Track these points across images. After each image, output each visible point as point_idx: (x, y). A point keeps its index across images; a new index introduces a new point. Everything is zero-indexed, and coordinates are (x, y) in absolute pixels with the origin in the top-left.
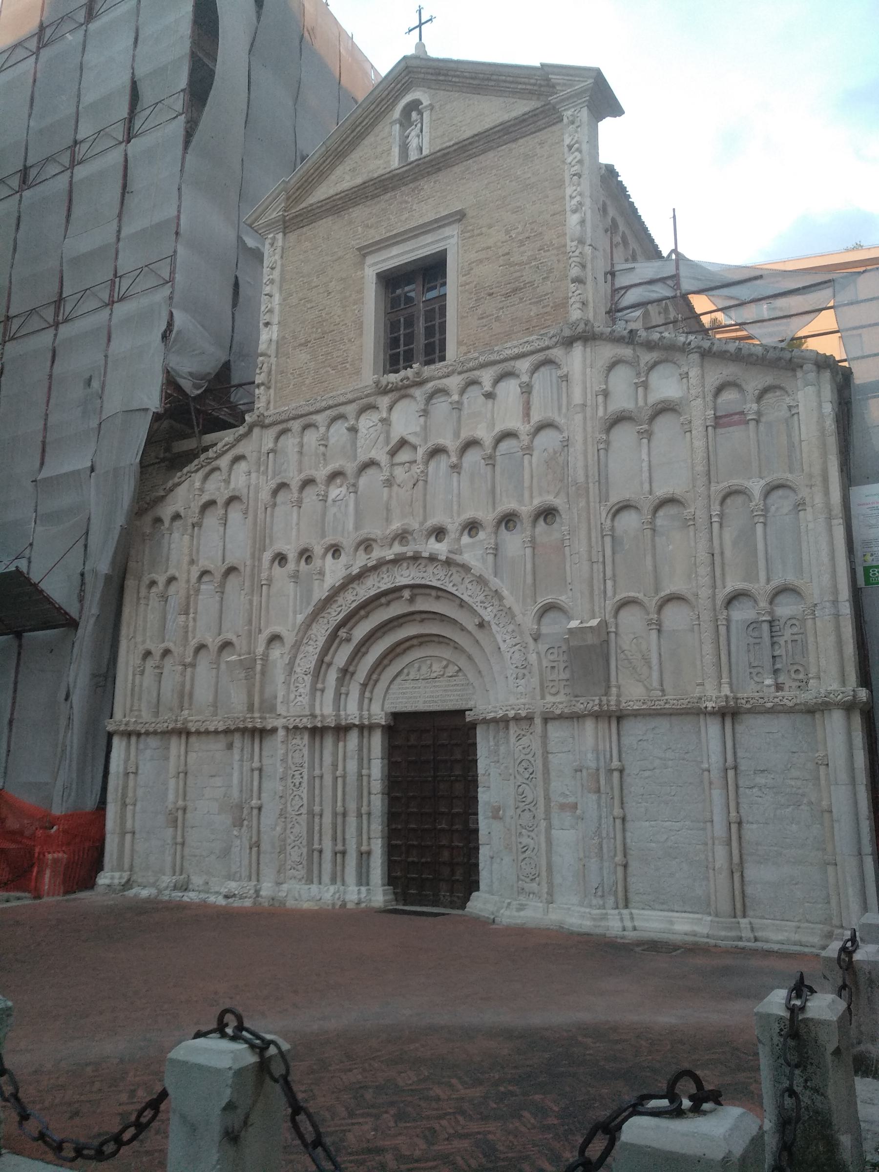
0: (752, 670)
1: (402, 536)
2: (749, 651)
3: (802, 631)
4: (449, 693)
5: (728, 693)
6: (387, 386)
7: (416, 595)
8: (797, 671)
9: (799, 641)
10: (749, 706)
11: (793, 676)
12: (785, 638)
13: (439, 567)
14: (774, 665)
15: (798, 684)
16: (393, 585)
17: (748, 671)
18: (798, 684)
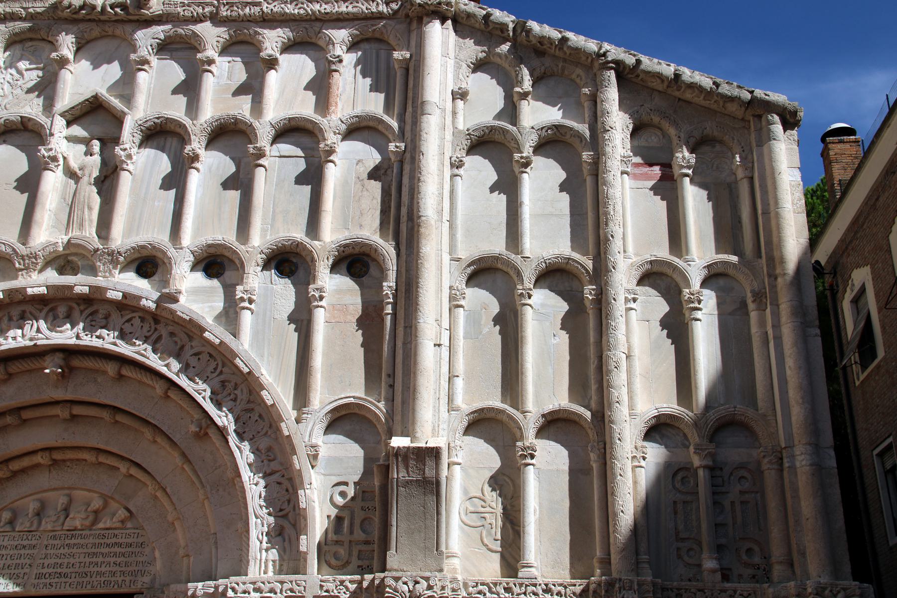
1: (67, 260)
2: (676, 513)
4: (100, 559)
6: (82, 7)
7: (72, 369)
11: (744, 557)
13: (137, 322)
16: (32, 343)
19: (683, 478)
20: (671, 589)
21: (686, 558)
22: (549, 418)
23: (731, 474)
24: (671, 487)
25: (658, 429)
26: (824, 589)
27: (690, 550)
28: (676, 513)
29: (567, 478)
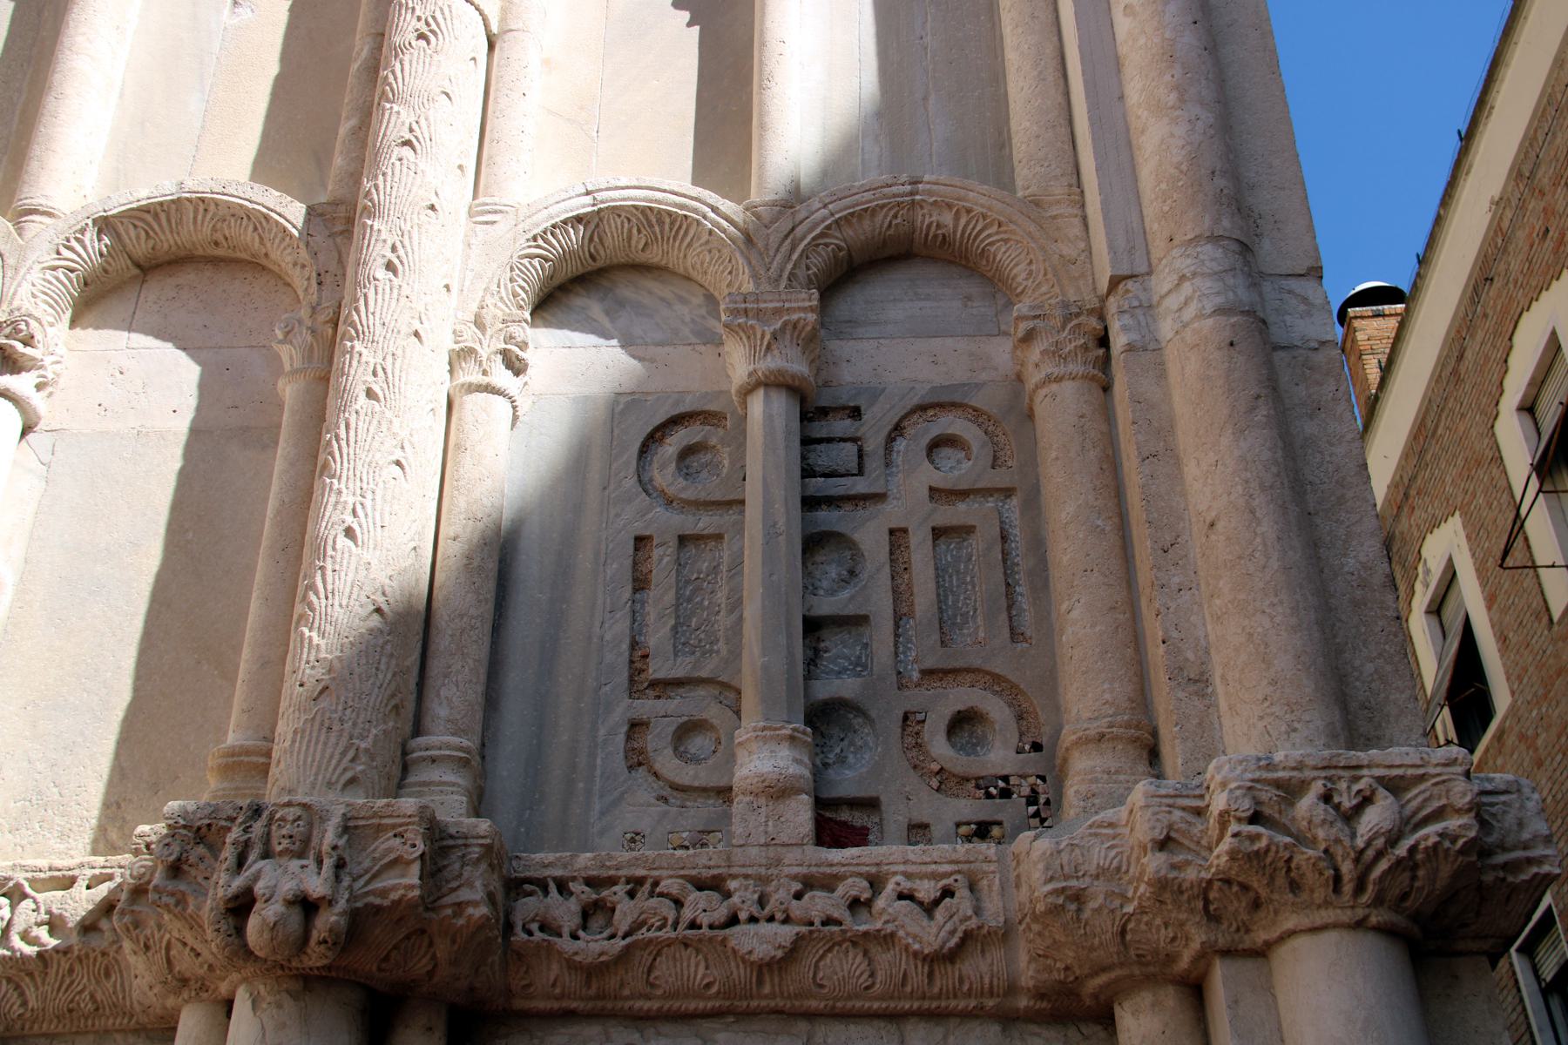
0: (646, 707)
2: (640, 583)
3: (1000, 479)
5: (452, 809)
8: (963, 723)
9: (986, 534)
10: (594, 946)
11: (940, 748)
12: (892, 513)
14: (809, 676)
15: (970, 808)
17: (624, 709)
18: (970, 808)
19: (687, 452)
20: (562, 887)
21: (667, 763)
22: (141, 249)
23: (898, 430)
24: (630, 482)
25: (590, 272)
26: (1291, 791)
27: (688, 729)
28: (640, 583)
29: (177, 464)
